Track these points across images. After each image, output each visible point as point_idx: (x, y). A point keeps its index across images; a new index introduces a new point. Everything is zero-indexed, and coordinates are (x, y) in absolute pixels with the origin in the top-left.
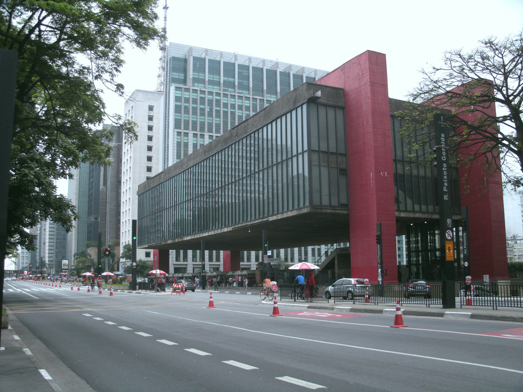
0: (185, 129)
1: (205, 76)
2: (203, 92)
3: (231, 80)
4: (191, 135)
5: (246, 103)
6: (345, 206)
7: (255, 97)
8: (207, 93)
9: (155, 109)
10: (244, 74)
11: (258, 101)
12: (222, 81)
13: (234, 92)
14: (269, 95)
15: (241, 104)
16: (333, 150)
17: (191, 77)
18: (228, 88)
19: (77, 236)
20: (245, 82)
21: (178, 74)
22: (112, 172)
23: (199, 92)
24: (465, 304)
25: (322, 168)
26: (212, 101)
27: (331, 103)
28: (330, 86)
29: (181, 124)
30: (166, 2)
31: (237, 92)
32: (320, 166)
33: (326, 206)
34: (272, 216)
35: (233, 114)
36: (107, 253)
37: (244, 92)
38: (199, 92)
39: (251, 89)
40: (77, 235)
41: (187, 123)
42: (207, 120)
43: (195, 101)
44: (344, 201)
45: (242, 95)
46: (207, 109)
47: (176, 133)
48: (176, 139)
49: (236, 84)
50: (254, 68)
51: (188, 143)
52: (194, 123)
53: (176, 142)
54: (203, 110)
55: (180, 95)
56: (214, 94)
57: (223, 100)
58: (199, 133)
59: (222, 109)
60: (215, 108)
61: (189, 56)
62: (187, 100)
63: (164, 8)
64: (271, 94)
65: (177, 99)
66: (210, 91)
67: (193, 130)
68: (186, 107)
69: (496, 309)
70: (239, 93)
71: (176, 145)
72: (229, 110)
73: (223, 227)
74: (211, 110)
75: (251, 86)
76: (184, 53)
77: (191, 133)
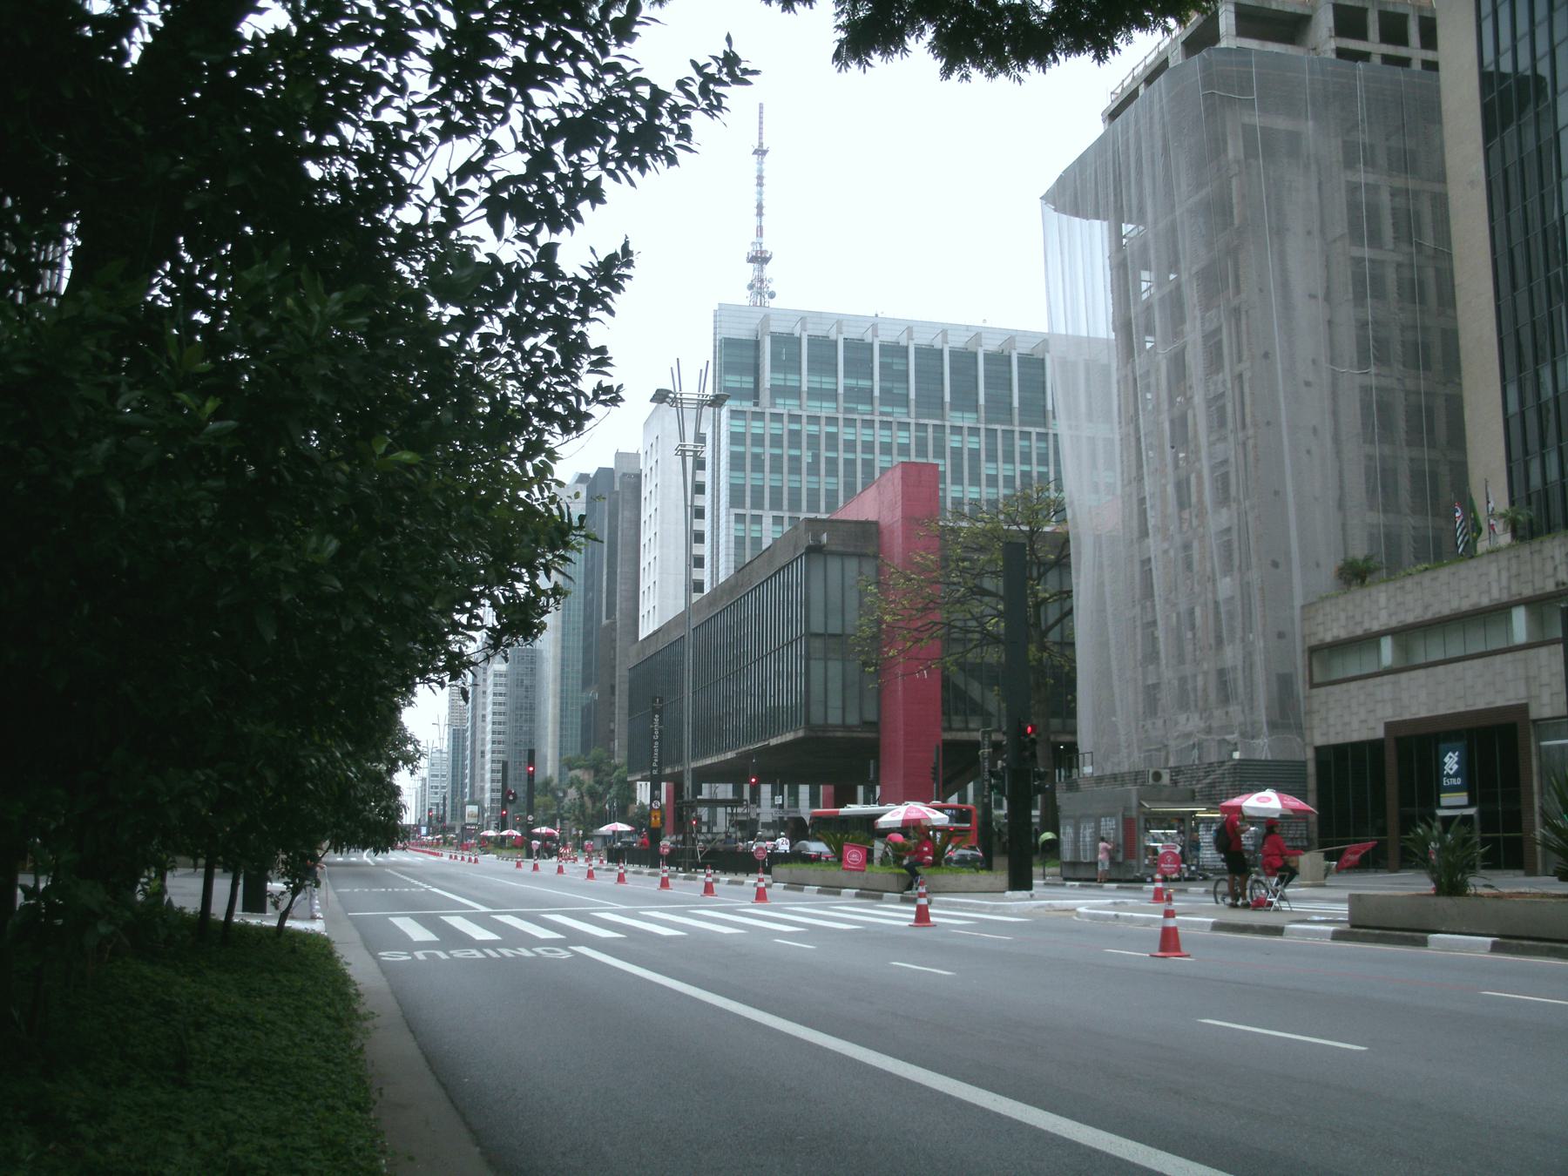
0: (753, 506)
1: (800, 381)
2: (795, 418)
3: (864, 383)
4: (767, 521)
5: (902, 437)
6: (865, 724)
7: (922, 421)
8: (804, 420)
10: (895, 367)
11: (930, 430)
12: (841, 390)
13: (872, 413)
14: (959, 414)
15: (888, 440)
17: (768, 385)
18: (858, 403)
19: (558, 737)
20: (898, 387)
21: (738, 378)
22: (623, 587)
23: (786, 419)
26: (817, 437)
27: (851, 550)
28: (850, 519)
29: (744, 497)
30: (760, 138)
31: (877, 412)
33: (837, 726)
35: (868, 464)
36: (511, 798)
37: (896, 410)
38: (786, 419)
39: (912, 404)
40: (558, 733)
41: (758, 492)
42: (805, 482)
43: (776, 441)
44: (871, 716)
45: (890, 419)
46: (807, 457)
47: (733, 518)
48: (732, 532)
49: (877, 393)
50: (918, 350)
51: (761, 538)
52: (776, 492)
53: (732, 538)
54: (796, 460)
55: (741, 430)
56: (823, 422)
57: (845, 434)
58: (786, 515)
59: (842, 456)
60: (824, 454)
61: (763, 335)
62: (758, 440)
63: (755, 152)
64: (963, 411)
65: (736, 438)
66: (813, 414)
67: (772, 508)
68: (756, 457)
70: (882, 414)
71: (732, 545)
72: (860, 456)
74: (816, 457)
75: (912, 395)
76: (753, 327)
77: (768, 516)
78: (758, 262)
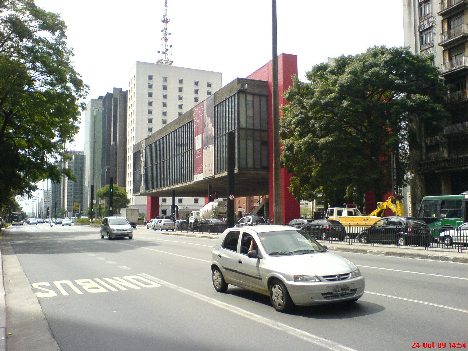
9: (154, 78)
16: (257, 127)
24: (402, 244)
25: (248, 141)
32: (246, 139)
33: (250, 168)
34: (217, 174)
44: (265, 164)
69: (351, 244)
73: (188, 181)
78: (165, 22)
